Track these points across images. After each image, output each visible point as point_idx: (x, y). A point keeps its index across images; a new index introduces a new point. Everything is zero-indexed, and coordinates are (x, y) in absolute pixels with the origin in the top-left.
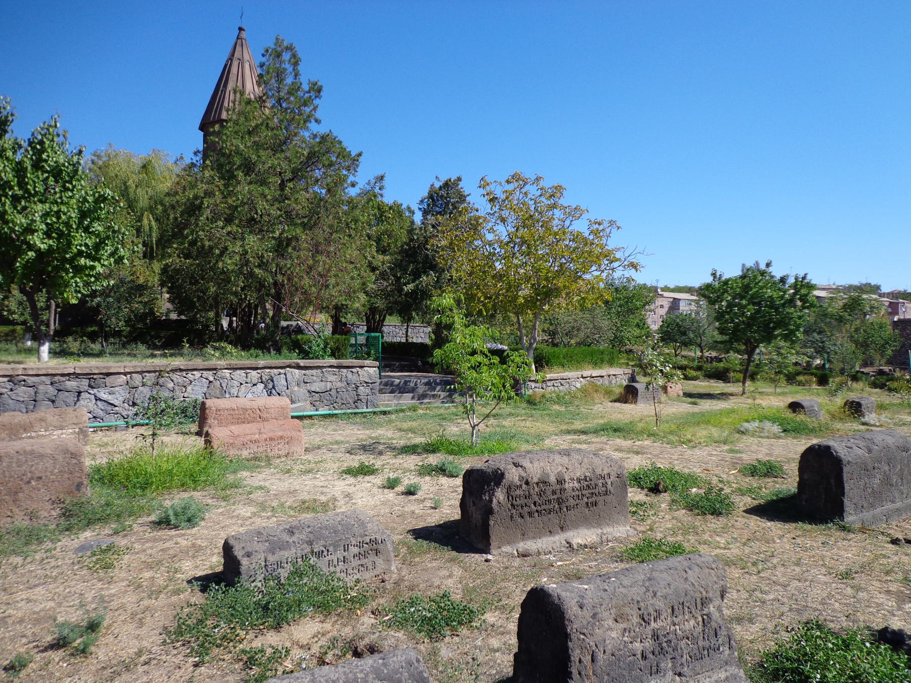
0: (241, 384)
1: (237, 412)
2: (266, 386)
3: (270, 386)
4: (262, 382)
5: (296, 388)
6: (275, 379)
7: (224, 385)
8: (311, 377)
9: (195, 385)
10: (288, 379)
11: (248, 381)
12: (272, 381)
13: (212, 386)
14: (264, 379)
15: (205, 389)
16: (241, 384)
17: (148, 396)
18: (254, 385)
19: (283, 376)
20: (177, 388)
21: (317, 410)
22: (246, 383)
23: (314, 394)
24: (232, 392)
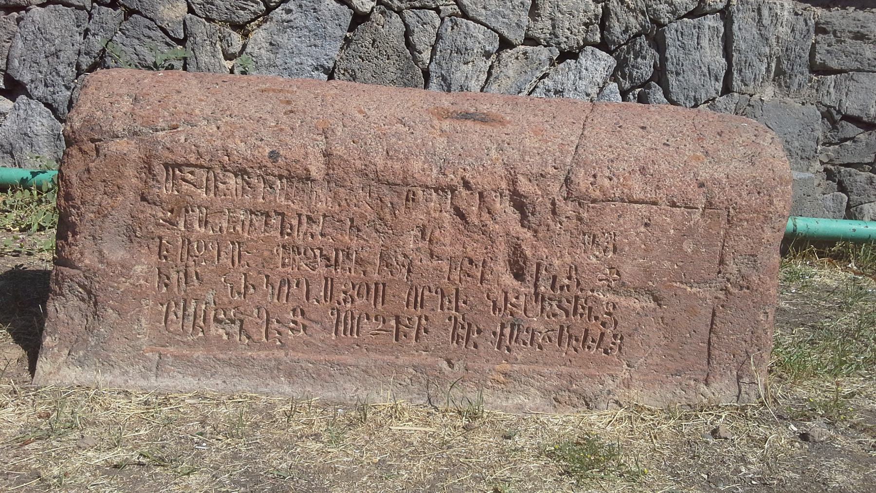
0: (505, 44)
1: (323, 201)
2: (622, 64)
3: (645, 68)
4: (603, 46)
5: (769, 92)
6: (670, 36)
7: (423, 39)
8: (850, 44)
9: (287, 25)
10: (739, 43)
11: (542, 28)
12: (659, 44)
13: (365, 35)
14: (617, 28)
15: (333, 51)
16: (505, 44)
17: (69, 54)
18: (565, 56)
19: (711, 22)
20: (200, 28)
21: (851, 213)
22: (531, 40)
23: (850, 129)
24: (458, 77)
